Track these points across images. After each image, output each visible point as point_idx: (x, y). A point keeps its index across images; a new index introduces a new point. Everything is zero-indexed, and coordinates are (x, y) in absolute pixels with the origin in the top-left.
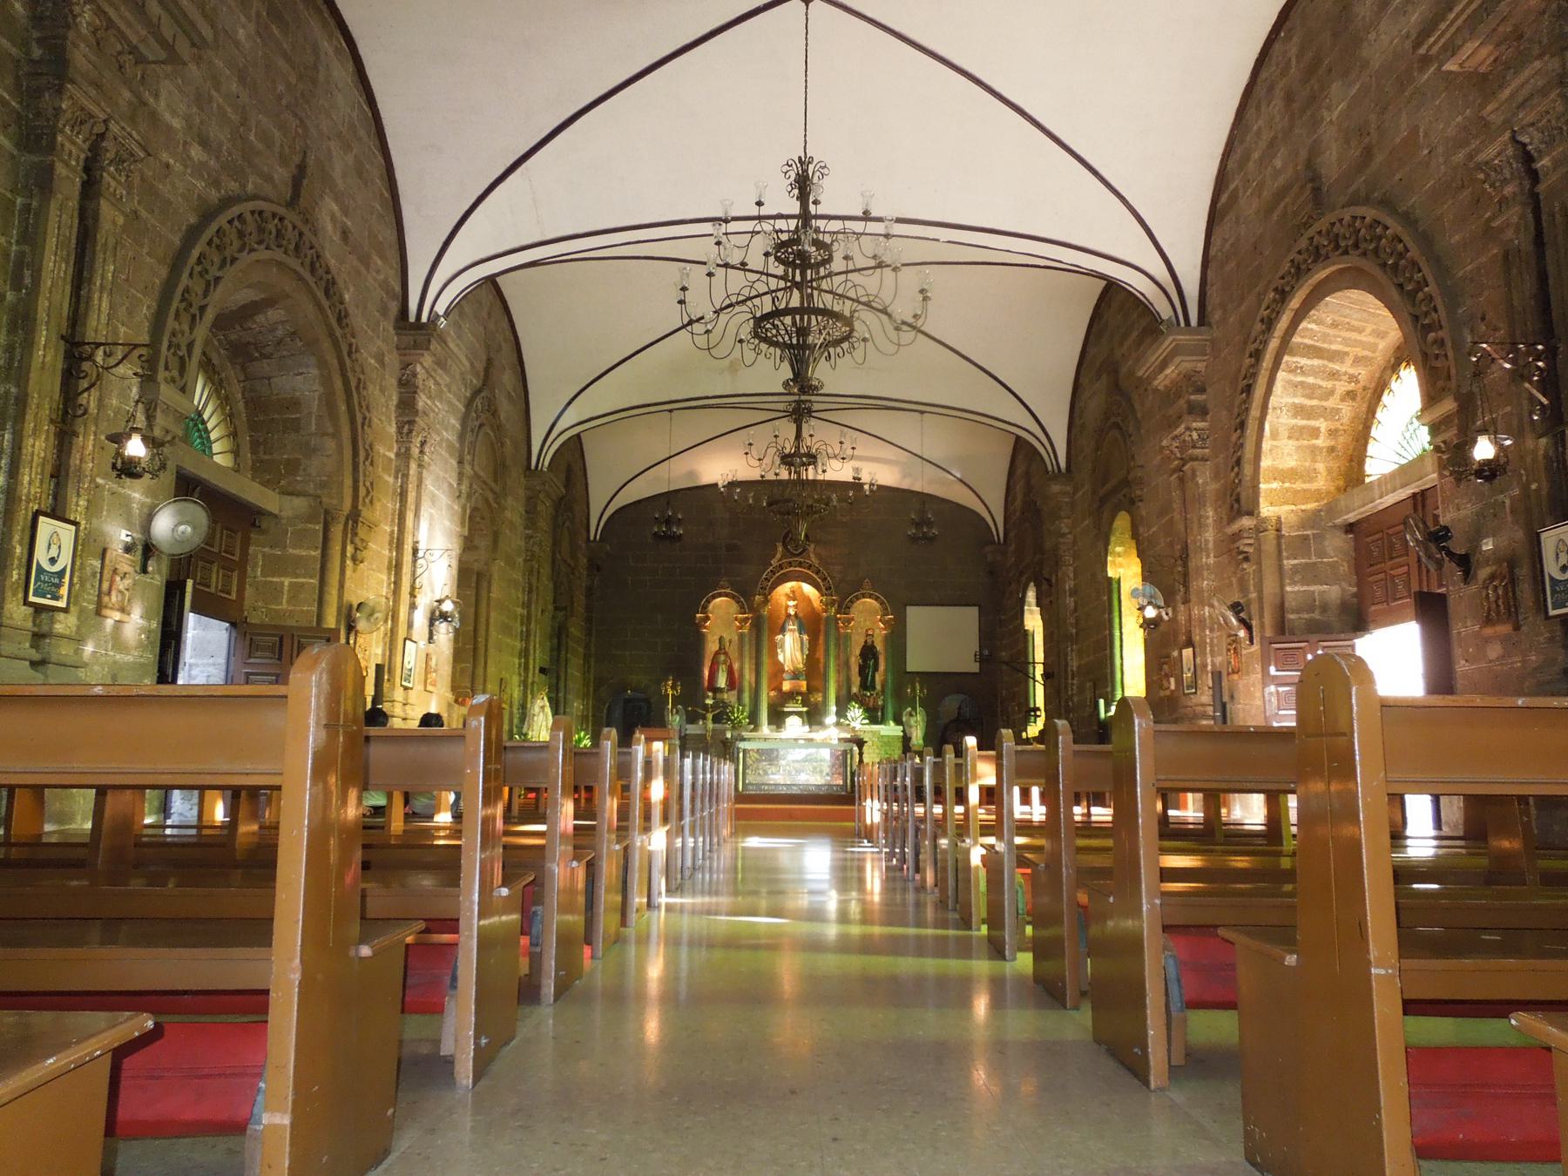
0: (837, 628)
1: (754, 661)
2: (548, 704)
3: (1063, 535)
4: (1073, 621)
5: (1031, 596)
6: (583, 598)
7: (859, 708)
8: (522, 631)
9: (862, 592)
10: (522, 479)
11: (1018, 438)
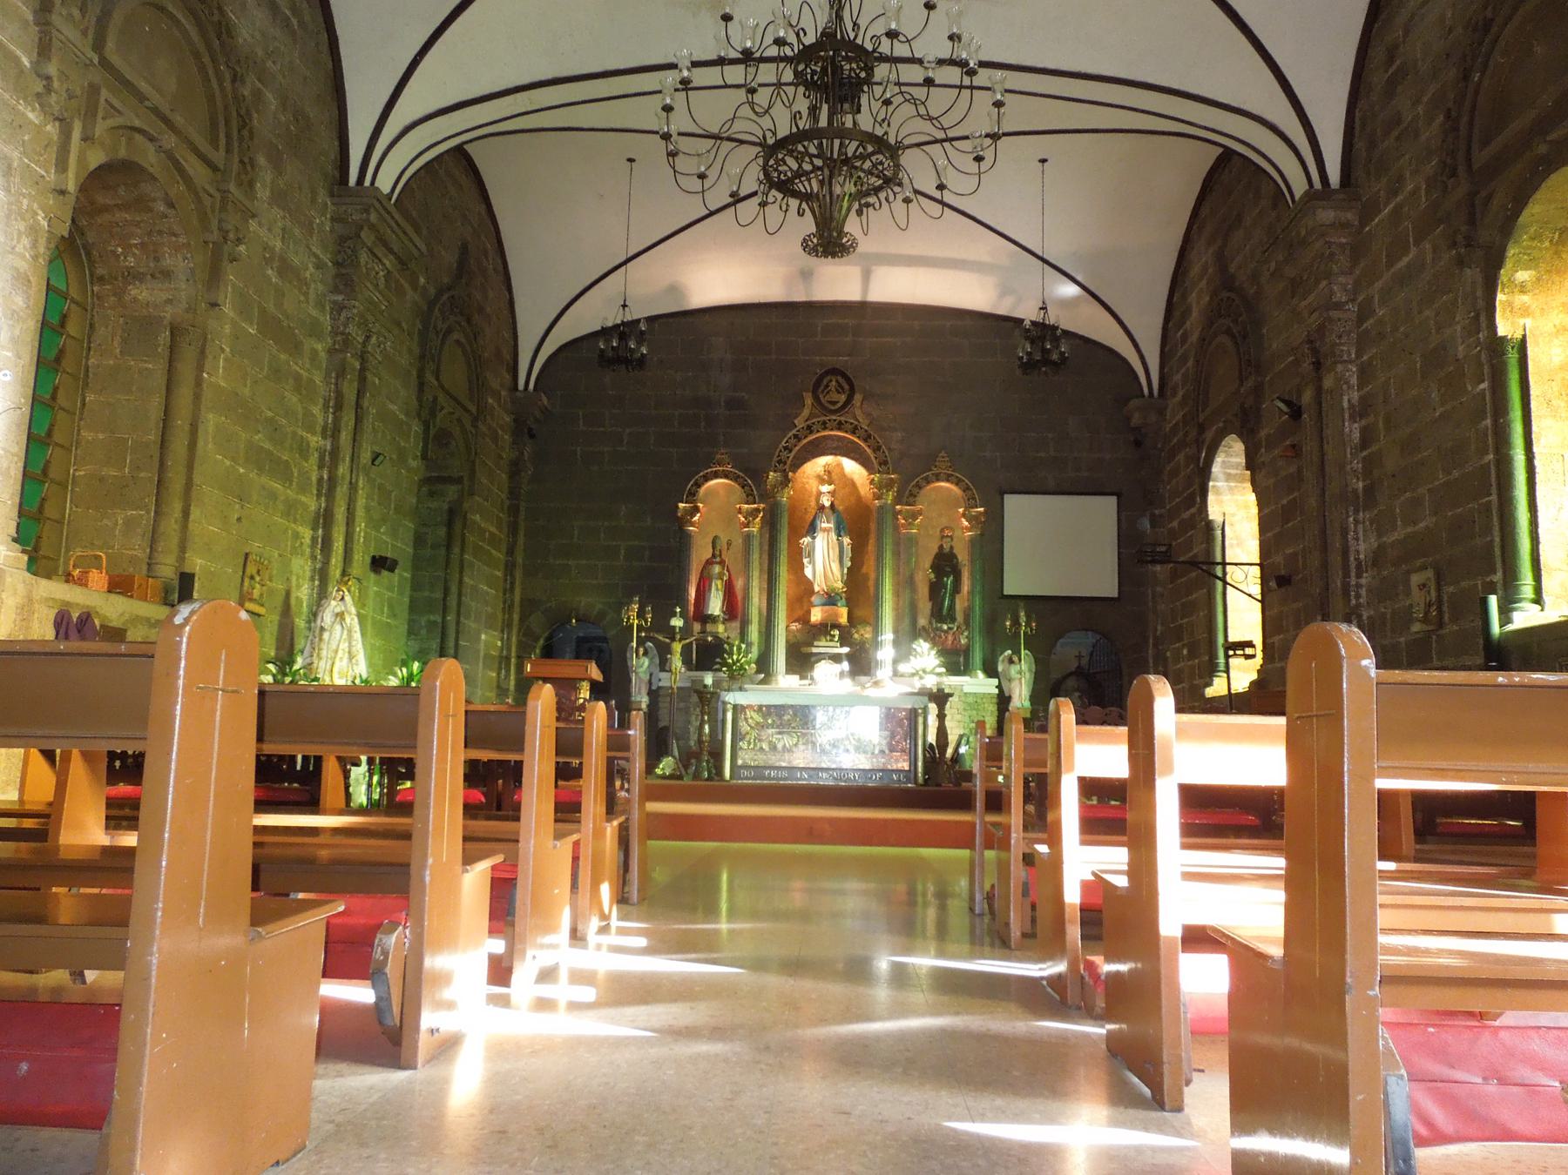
0: (896, 528)
1: (766, 577)
2: (353, 610)
3: (1338, 306)
4: (1357, 465)
5: (1229, 460)
7: (932, 648)
8: (320, 480)
9: (935, 470)
10: (322, 196)
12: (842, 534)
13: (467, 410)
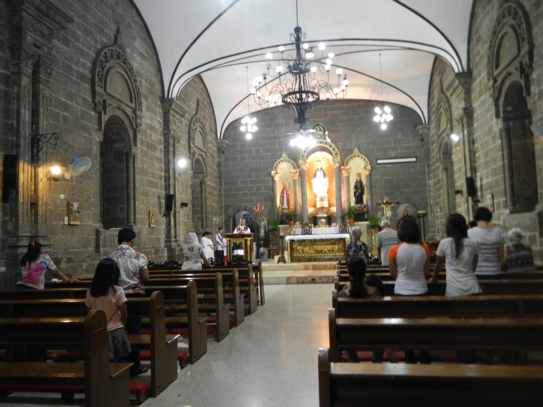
6: (216, 167)
11: (437, 58)
12: (325, 177)
13: (203, 151)
